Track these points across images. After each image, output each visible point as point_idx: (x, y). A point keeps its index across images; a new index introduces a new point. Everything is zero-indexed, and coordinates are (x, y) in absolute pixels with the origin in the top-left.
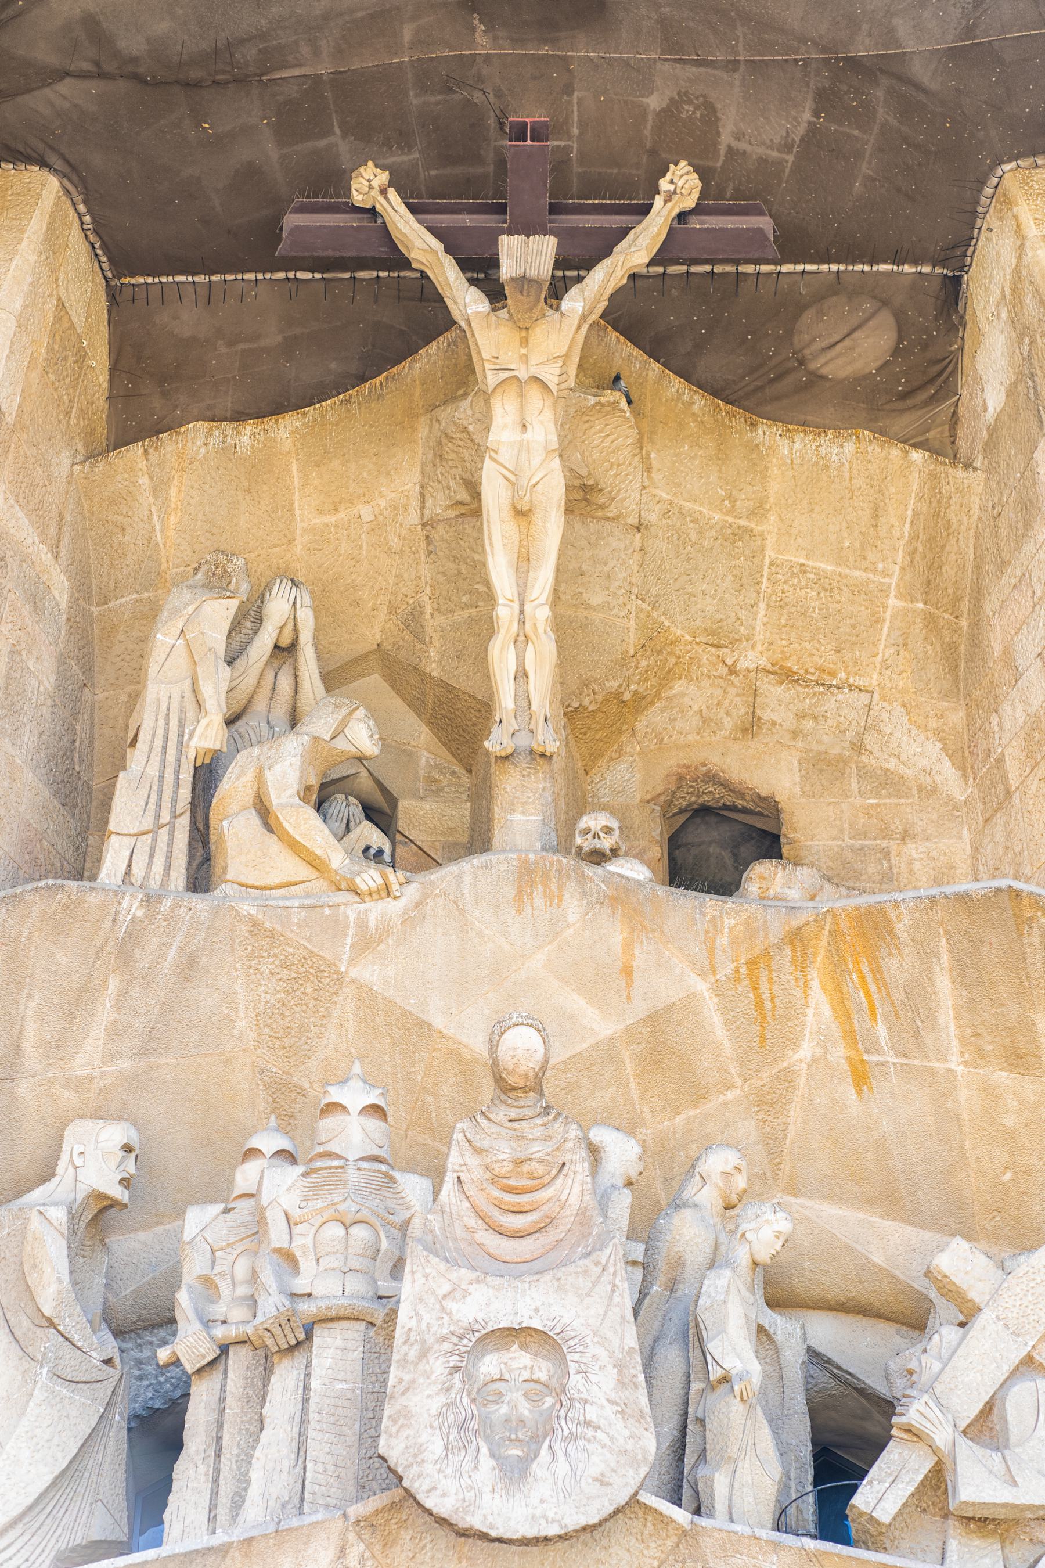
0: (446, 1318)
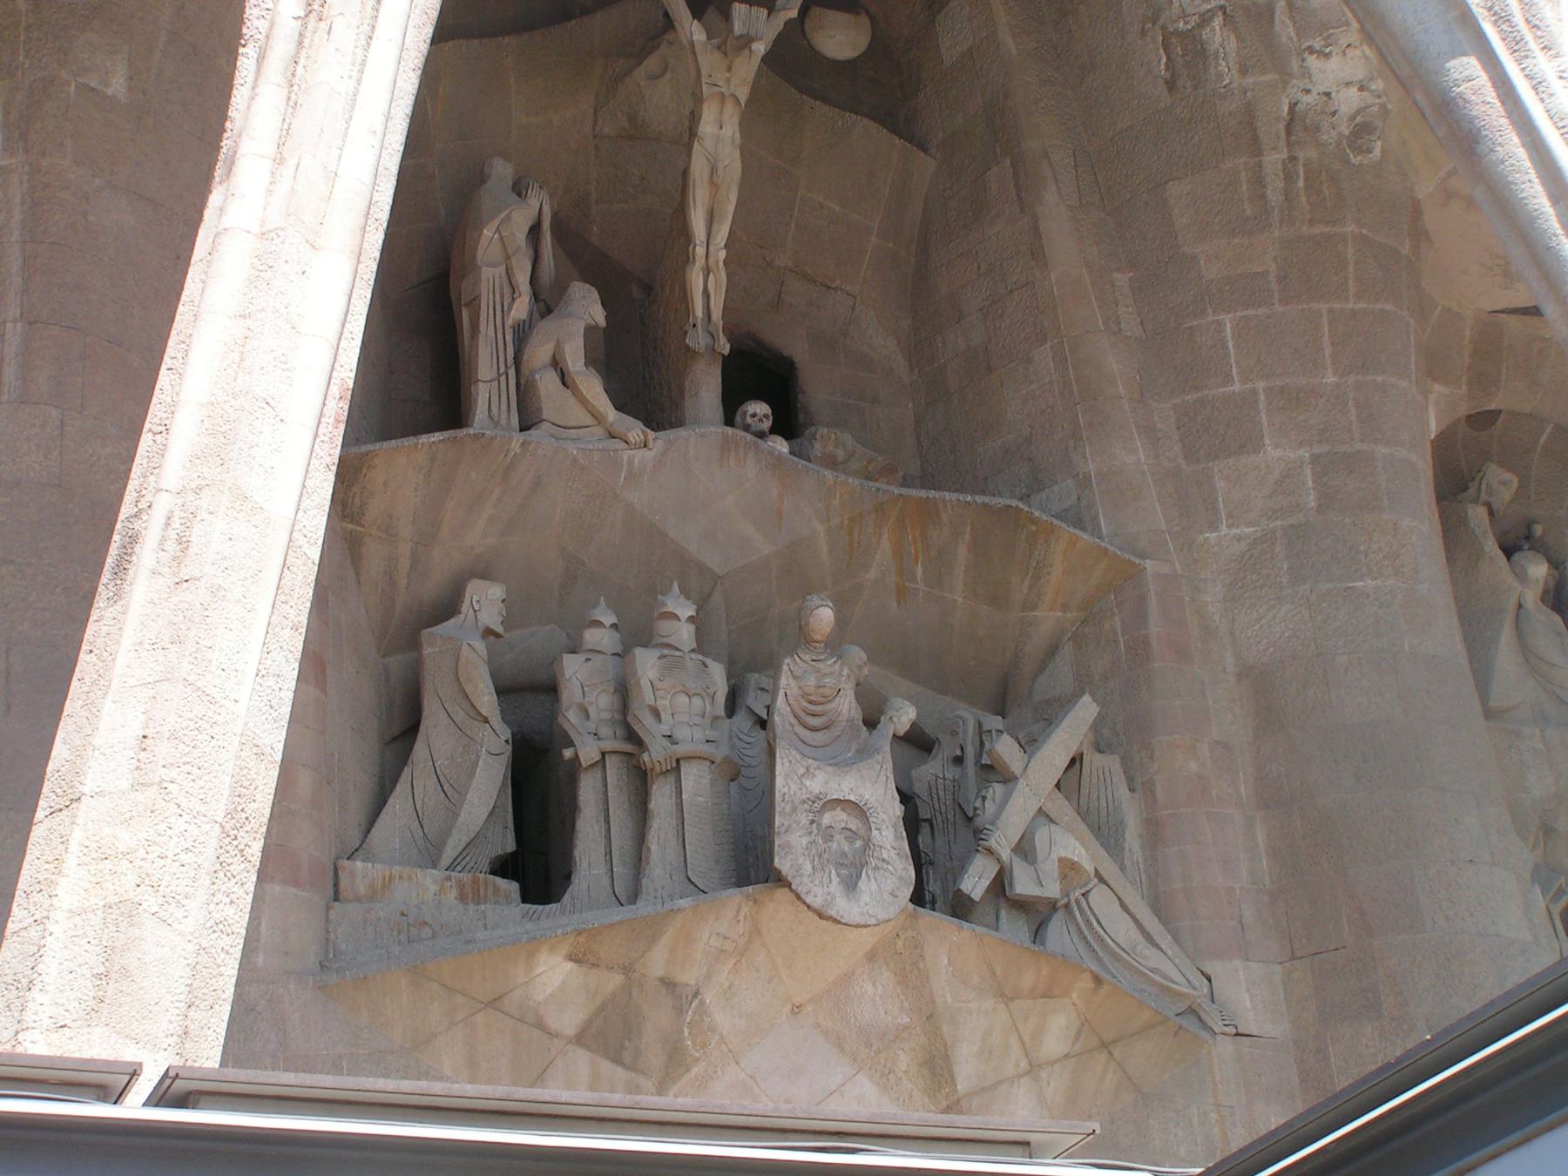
0: (804, 789)
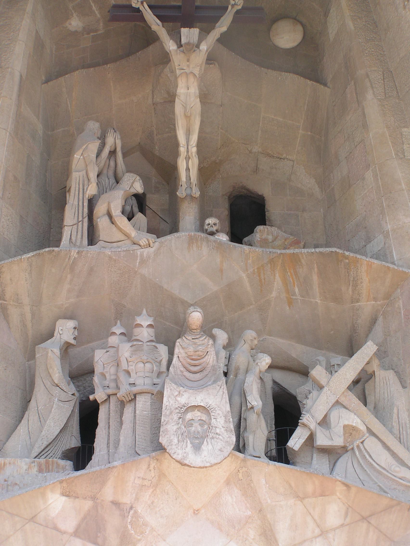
0: (176, 402)
